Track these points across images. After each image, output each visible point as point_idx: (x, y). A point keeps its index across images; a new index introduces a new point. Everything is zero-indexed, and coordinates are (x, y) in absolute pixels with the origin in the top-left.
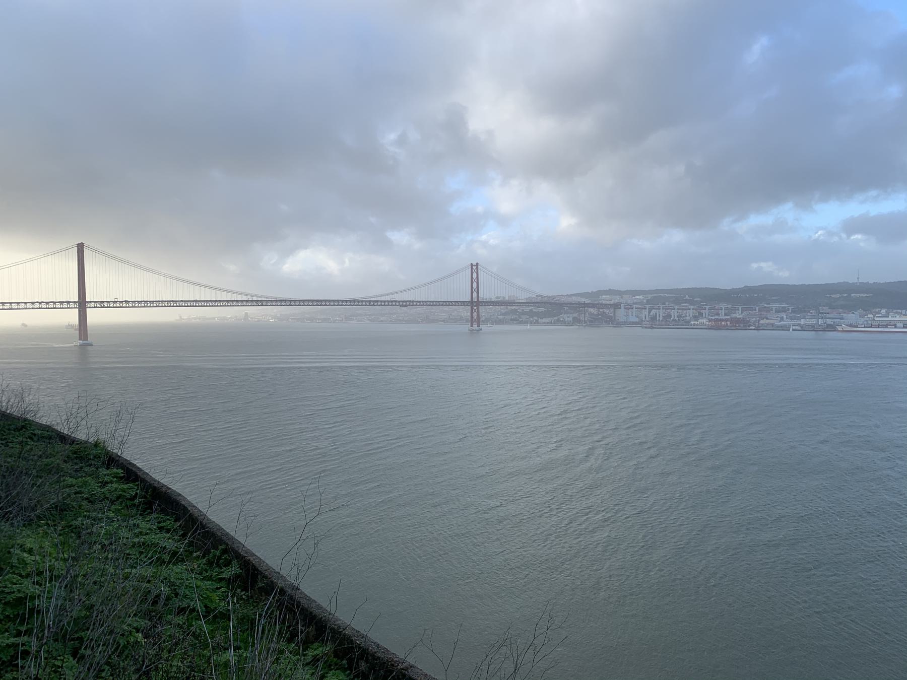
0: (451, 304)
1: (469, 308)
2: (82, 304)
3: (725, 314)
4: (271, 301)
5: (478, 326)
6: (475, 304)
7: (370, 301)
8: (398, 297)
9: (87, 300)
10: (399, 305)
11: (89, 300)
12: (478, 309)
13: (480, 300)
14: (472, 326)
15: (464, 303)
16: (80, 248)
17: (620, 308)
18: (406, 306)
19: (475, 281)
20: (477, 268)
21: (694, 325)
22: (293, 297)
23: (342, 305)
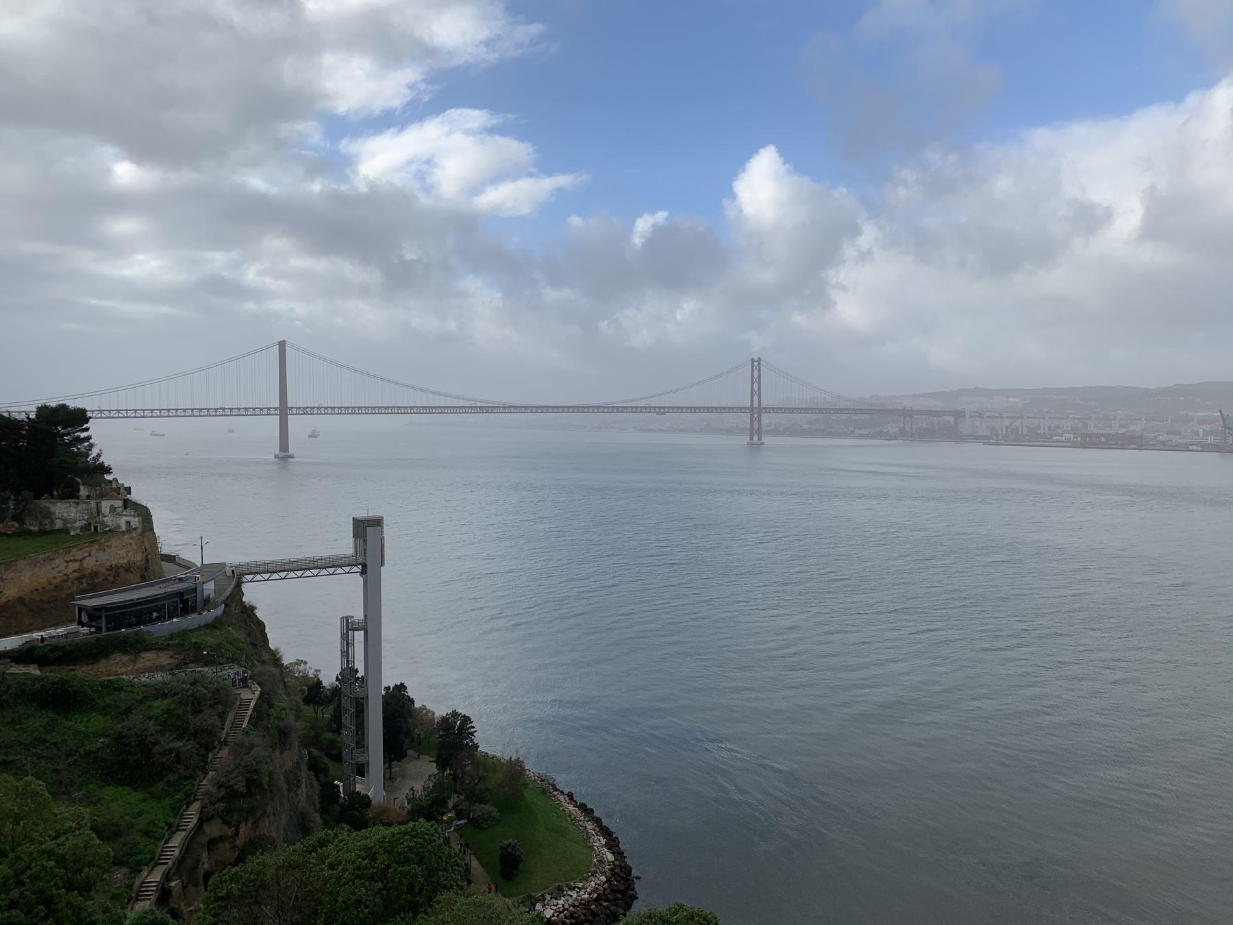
1: (749, 414)
2: (283, 411)
3: (1121, 426)
5: (760, 439)
6: (756, 411)
7: (618, 407)
9: (289, 405)
12: (759, 417)
13: (762, 406)
14: (752, 439)
15: (740, 410)
16: (282, 345)
17: (964, 417)
18: (664, 413)
19: (756, 381)
20: (759, 364)
21: (1057, 442)
22: (524, 403)
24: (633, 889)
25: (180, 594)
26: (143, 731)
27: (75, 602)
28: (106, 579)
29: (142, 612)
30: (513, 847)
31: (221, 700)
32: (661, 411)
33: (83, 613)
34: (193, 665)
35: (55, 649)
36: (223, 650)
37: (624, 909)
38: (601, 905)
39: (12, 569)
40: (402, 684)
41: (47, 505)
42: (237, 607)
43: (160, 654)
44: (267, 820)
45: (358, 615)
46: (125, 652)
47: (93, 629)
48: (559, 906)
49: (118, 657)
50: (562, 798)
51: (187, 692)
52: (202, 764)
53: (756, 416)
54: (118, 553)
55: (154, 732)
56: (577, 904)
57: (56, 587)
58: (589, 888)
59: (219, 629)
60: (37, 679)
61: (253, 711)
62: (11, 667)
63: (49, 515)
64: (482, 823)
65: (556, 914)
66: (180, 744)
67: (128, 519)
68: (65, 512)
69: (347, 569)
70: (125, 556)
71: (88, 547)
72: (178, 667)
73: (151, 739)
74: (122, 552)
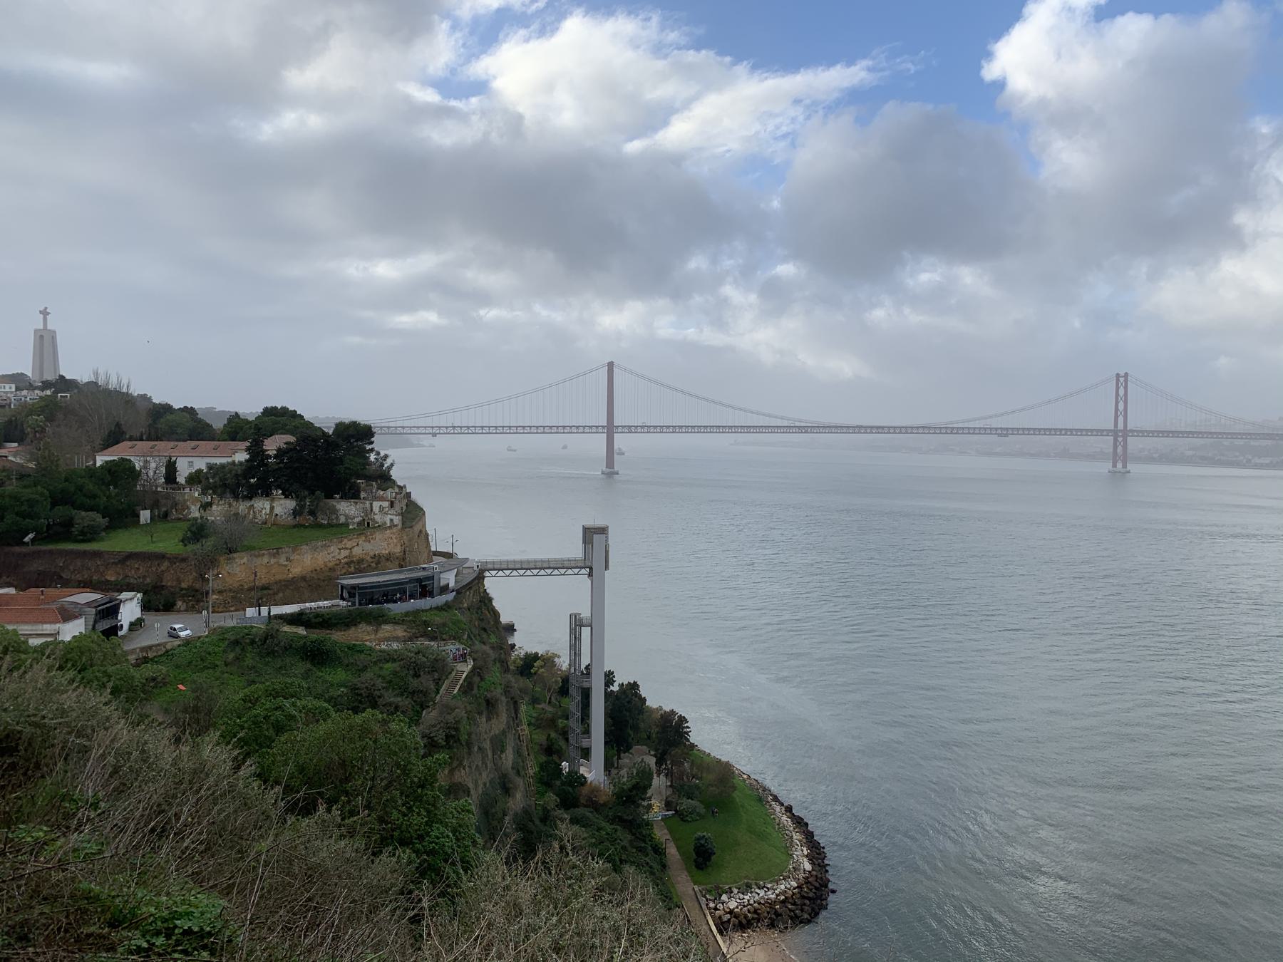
0: (1171, 435)
1: (1112, 438)
2: (610, 429)
4: (818, 427)
5: (1124, 466)
6: (1120, 435)
7: (953, 428)
8: (995, 423)
10: (995, 434)
11: (617, 425)
12: (1125, 441)
13: (1128, 429)
14: (1114, 466)
15: (1100, 432)
16: (611, 365)
18: (1006, 435)
20: (1126, 381)
23: (907, 433)
24: (826, 899)
25: (419, 580)
26: (372, 686)
27: (339, 581)
28: (370, 566)
29: (390, 593)
30: (706, 839)
31: (439, 669)
32: (1004, 432)
33: (344, 591)
34: (422, 639)
35: (317, 615)
36: (447, 629)
37: (810, 915)
38: (786, 907)
39: (298, 552)
40: (635, 683)
41: (334, 504)
42: (475, 597)
43: (396, 627)
44: (463, 771)
45: (585, 613)
46: (369, 623)
47: (350, 604)
48: (744, 900)
49: (364, 627)
50: (778, 808)
51: (411, 659)
52: (416, 718)
53: (1120, 439)
54: (381, 544)
55: (380, 687)
56: (762, 901)
57: (330, 569)
58: (778, 890)
59: (446, 611)
60: (302, 637)
61: (464, 681)
62: (284, 626)
63: (334, 511)
64: (687, 816)
65: (740, 907)
66: (399, 699)
67: (392, 517)
68: (347, 509)
69: (576, 571)
70: (386, 547)
71: (357, 538)
72: (410, 639)
73: (377, 693)
74: (385, 544)
